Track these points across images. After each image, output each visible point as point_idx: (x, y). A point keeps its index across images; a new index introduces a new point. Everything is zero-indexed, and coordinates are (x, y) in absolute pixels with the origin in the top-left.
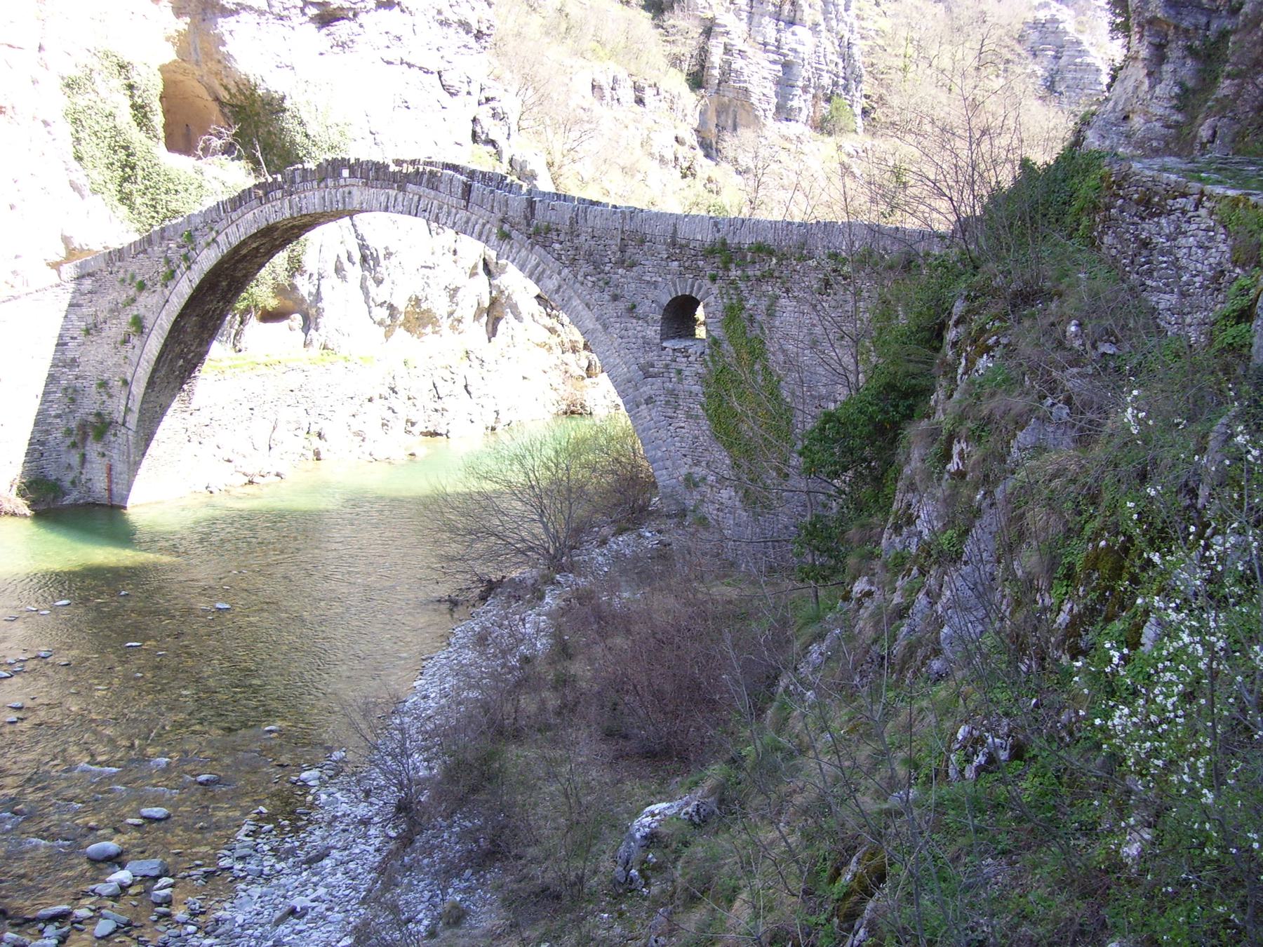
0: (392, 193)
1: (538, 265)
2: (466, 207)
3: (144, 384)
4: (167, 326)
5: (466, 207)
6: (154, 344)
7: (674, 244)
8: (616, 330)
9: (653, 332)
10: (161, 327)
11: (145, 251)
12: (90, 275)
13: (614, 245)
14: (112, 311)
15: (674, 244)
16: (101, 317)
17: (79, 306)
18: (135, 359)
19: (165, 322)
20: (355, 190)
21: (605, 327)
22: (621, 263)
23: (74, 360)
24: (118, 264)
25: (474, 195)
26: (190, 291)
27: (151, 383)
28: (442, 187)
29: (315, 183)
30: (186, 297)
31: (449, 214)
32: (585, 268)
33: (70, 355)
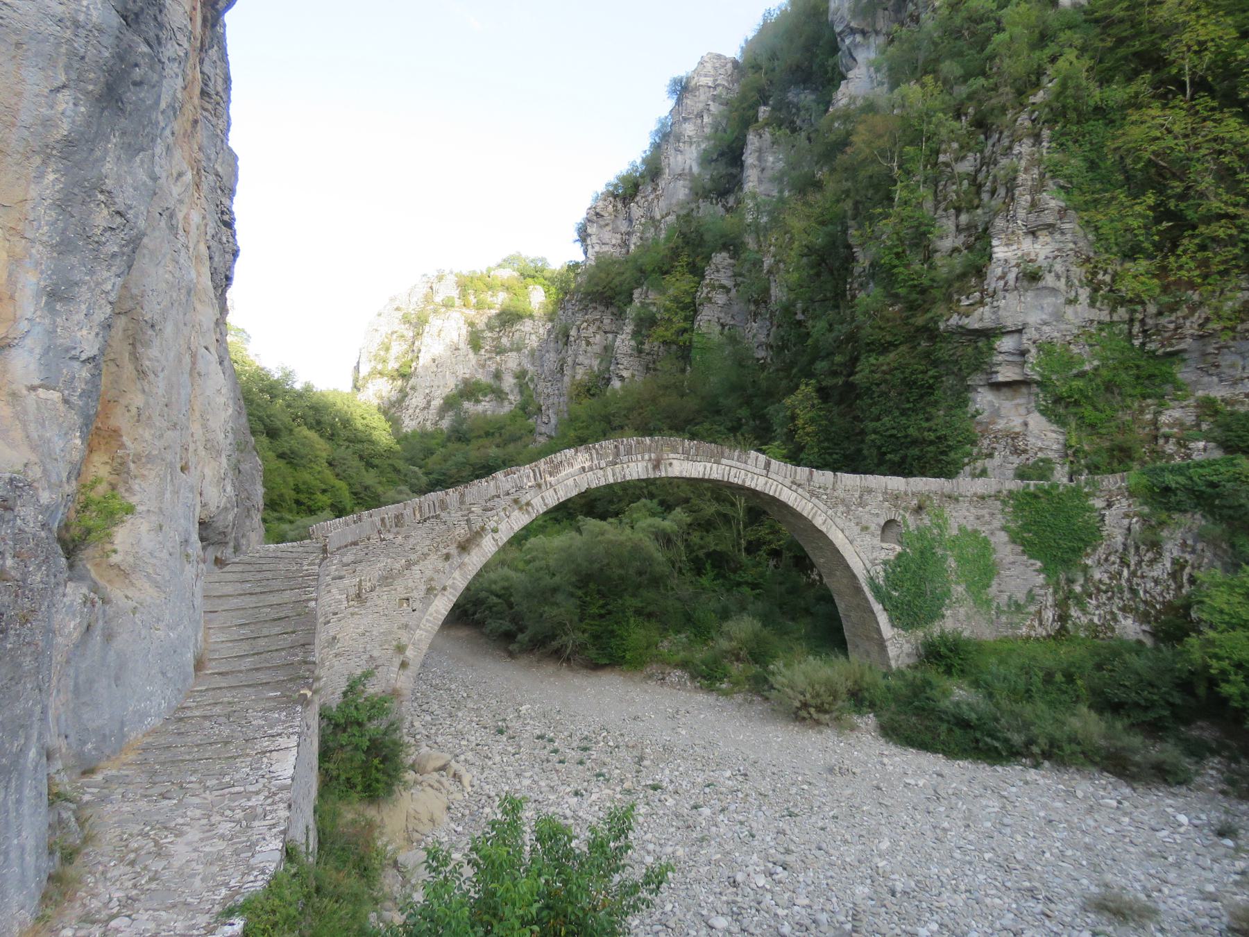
0: (709, 465)
3: (425, 647)
7: (886, 493)
8: (858, 542)
9: (877, 541)
10: (453, 587)
11: (437, 517)
12: (355, 544)
13: (857, 495)
15: (886, 493)
17: (341, 578)
20: (675, 462)
21: (851, 542)
22: (860, 505)
23: (334, 638)
24: (394, 530)
26: (495, 549)
29: (639, 457)
30: (490, 555)
32: (841, 508)
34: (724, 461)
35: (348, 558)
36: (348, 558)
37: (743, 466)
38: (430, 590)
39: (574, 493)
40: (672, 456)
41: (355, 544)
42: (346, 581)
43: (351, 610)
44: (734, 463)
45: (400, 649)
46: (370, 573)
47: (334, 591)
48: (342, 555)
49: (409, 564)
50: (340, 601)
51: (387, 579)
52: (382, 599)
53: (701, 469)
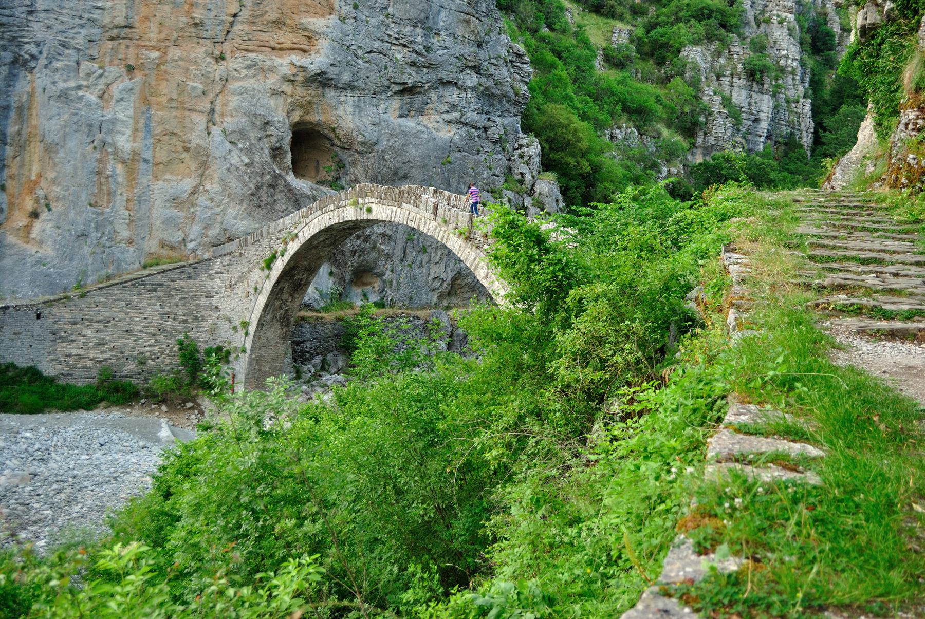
0: (394, 208)
1: (475, 259)
2: (435, 219)
4: (269, 289)
5: (435, 219)
6: (262, 300)
12: (229, 254)
14: (240, 277)
16: (234, 280)
17: (222, 273)
18: (251, 309)
19: (268, 286)
20: (374, 207)
23: (217, 307)
25: (439, 211)
27: (260, 325)
28: (422, 205)
31: (425, 223)
33: (215, 304)
34: (404, 205)
35: (226, 262)
36: (226, 262)
37: (417, 209)
38: (256, 289)
39: (317, 230)
40: (371, 200)
41: (229, 254)
42: (225, 276)
43: (227, 293)
44: (410, 207)
45: (245, 325)
46: (236, 271)
47: (217, 280)
48: (223, 260)
49: (250, 271)
50: (221, 287)
51: (242, 278)
52: (240, 291)
53: (389, 212)
